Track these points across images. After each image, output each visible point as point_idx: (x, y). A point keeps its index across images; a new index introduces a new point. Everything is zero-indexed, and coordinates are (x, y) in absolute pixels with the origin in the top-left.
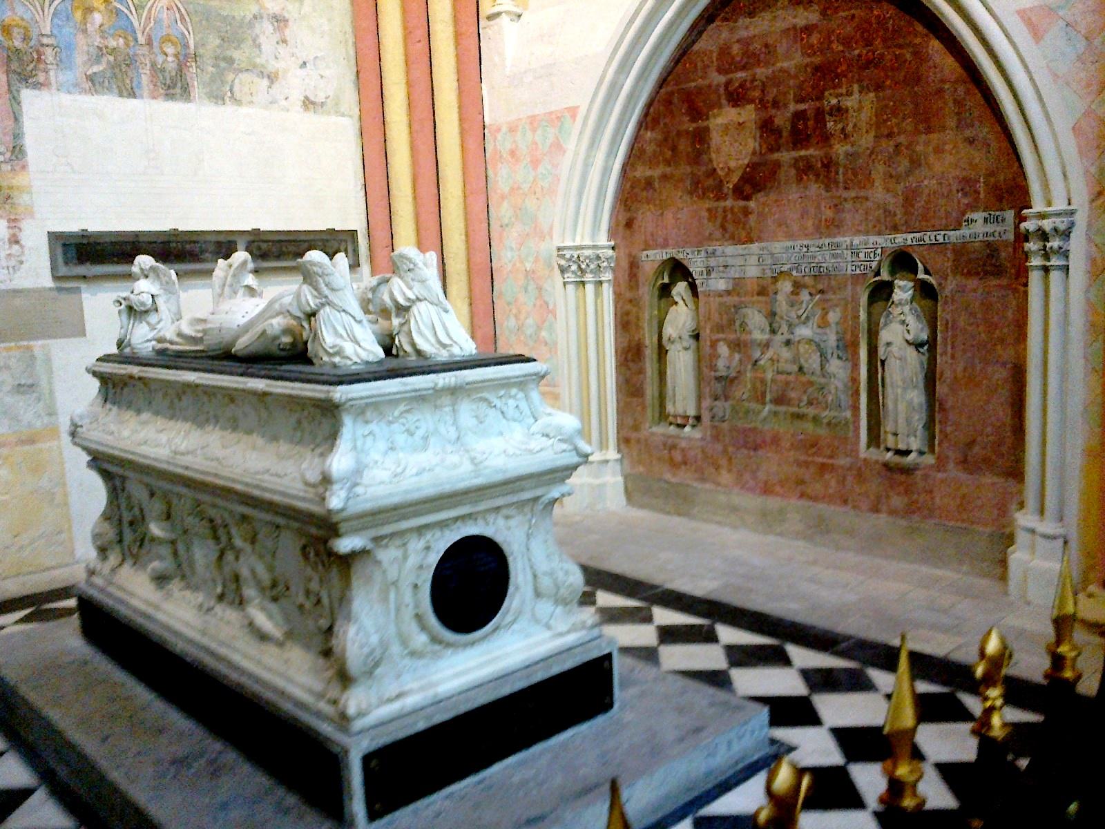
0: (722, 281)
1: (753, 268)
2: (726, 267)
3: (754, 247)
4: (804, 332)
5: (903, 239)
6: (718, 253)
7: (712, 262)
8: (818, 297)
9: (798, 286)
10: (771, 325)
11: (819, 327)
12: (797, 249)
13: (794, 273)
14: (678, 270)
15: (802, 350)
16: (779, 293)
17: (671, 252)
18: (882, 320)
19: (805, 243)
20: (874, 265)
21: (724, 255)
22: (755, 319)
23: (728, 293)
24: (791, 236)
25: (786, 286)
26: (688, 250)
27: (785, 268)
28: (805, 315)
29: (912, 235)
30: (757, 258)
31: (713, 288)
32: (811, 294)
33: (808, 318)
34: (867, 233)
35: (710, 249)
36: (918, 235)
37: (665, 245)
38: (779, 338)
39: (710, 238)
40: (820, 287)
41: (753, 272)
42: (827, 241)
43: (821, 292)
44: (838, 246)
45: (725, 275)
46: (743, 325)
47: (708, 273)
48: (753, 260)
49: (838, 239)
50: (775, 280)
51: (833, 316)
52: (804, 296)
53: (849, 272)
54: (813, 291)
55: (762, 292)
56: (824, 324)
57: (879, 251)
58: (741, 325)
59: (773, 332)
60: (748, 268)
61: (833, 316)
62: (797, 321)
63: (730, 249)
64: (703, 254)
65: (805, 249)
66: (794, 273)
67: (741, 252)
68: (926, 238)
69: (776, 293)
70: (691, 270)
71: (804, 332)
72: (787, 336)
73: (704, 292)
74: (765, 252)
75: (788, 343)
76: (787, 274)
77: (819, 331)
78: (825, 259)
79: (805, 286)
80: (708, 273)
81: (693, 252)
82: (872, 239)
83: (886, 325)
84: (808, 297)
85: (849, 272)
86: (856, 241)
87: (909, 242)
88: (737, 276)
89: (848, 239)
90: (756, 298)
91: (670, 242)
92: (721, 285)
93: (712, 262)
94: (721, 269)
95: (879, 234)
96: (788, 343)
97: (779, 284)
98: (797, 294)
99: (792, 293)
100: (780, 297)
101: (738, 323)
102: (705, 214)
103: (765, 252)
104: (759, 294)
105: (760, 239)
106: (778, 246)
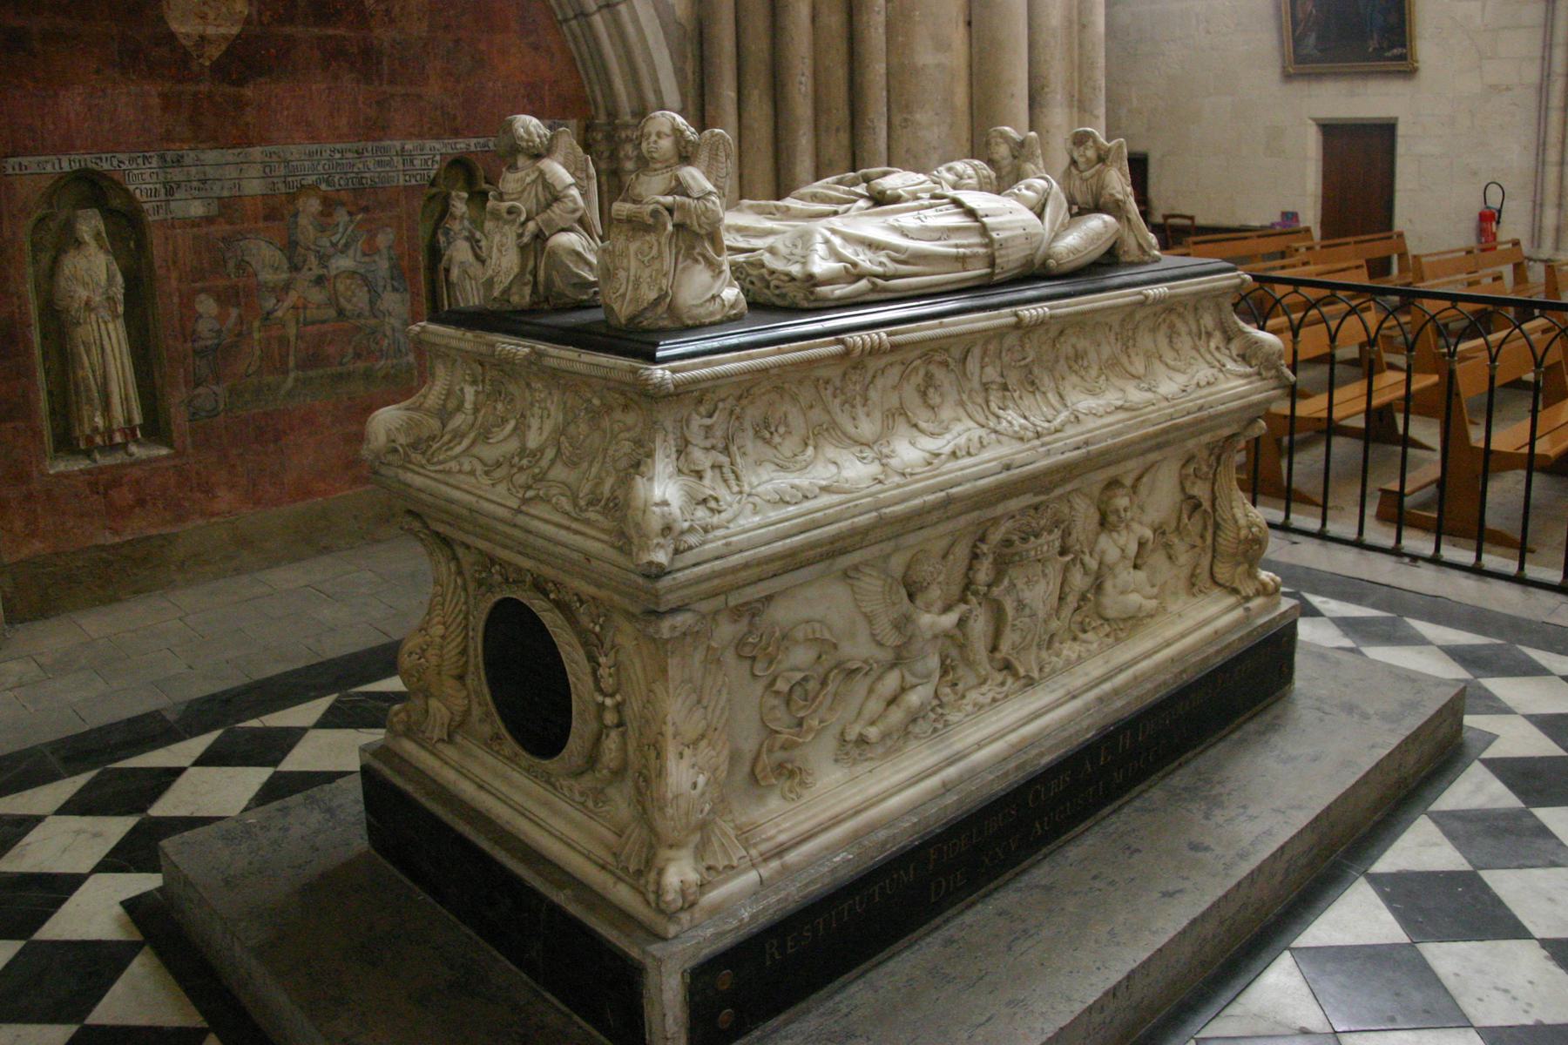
0: (197, 203)
1: (256, 182)
2: (204, 181)
3: (256, 152)
4: (344, 263)
5: (461, 145)
6: (187, 161)
7: (177, 175)
8: (359, 217)
9: (329, 205)
10: (290, 259)
11: (365, 255)
12: (326, 155)
13: (323, 187)
14: (94, 189)
15: (341, 287)
16: (301, 215)
17: (67, 164)
18: (442, 239)
19: (338, 146)
20: (432, 174)
21: (199, 163)
22: (264, 257)
23: (209, 220)
24: (313, 138)
25: (313, 205)
26: (120, 156)
27: (310, 180)
28: (343, 241)
29: (474, 141)
30: (259, 167)
31: (180, 215)
32: (350, 214)
33: (347, 246)
34: (421, 136)
35: (170, 156)
36: (482, 140)
37: (67, 147)
38: (306, 275)
39: (168, 137)
40: (363, 203)
41: (254, 186)
42: (370, 145)
43: (366, 209)
44: (385, 150)
45: (203, 194)
46: (242, 265)
47: (170, 192)
48: (256, 171)
49: (387, 143)
50: (292, 198)
51: (384, 239)
52: (341, 216)
53: (402, 182)
54: (354, 209)
55: (272, 215)
56: (371, 251)
57: (438, 158)
58: (238, 267)
59: (295, 268)
60: (244, 183)
61: (384, 239)
62: (332, 250)
63: (211, 156)
64: (155, 162)
65: (338, 156)
66: (323, 187)
67: (231, 159)
68: (491, 144)
69: (296, 215)
70: (131, 188)
71: (344, 263)
72: (317, 271)
73: (162, 222)
74: (275, 158)
75: (320, 281)
76: (314, 187)
77: (366, 259)
78: (370, 168)
79: (343, 204)
80: (170, 192)
81: (131, 160)
82: (429, 144)
83: (449, 243)
84: (347, 218)
85: (402, 182)
86: (409, 146)
87: (473, 148)
88: (226, 193)
89: (398, 144)
90: (261, 224)
91: (78, 143)
92: (197, 209)
93: (177, 175)
94: (195, 184)
95: (437, 137)
96: (320, 281)
97: (300, 203)
98: (330, 215)
99: (322, 213)
100: (303, 220)
101: (231, 264)
102: (155, 101)
103: (275, 158)
104: (266, 218)
105: (264, 141)
106: (295, 152)
